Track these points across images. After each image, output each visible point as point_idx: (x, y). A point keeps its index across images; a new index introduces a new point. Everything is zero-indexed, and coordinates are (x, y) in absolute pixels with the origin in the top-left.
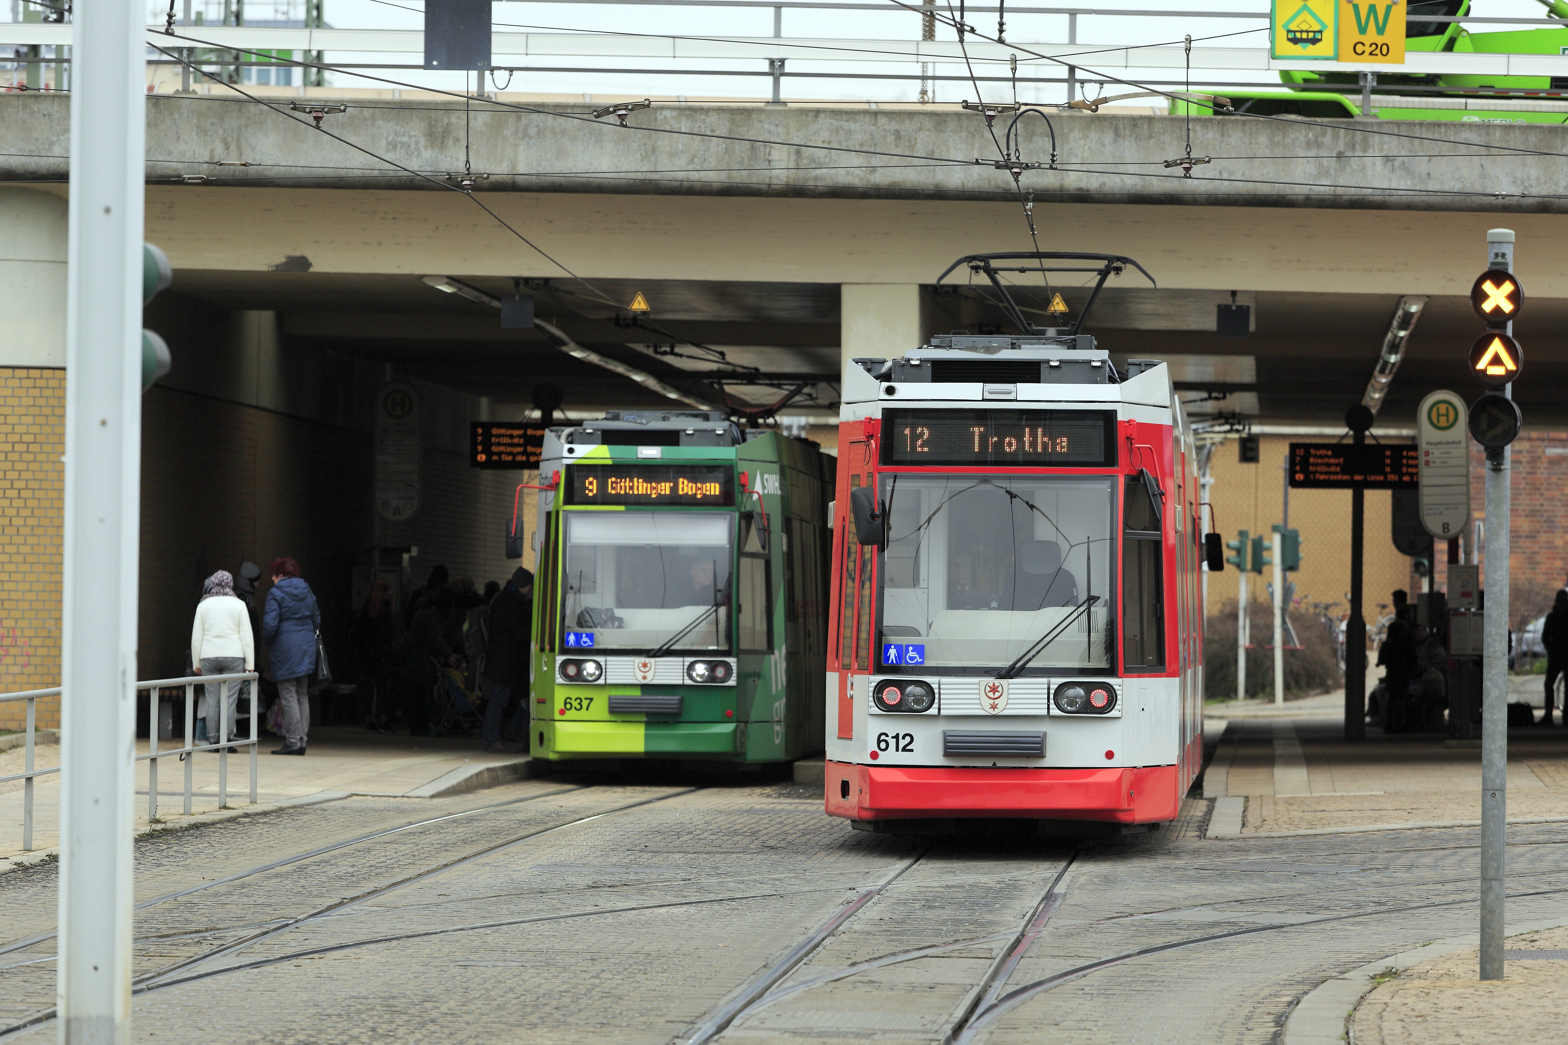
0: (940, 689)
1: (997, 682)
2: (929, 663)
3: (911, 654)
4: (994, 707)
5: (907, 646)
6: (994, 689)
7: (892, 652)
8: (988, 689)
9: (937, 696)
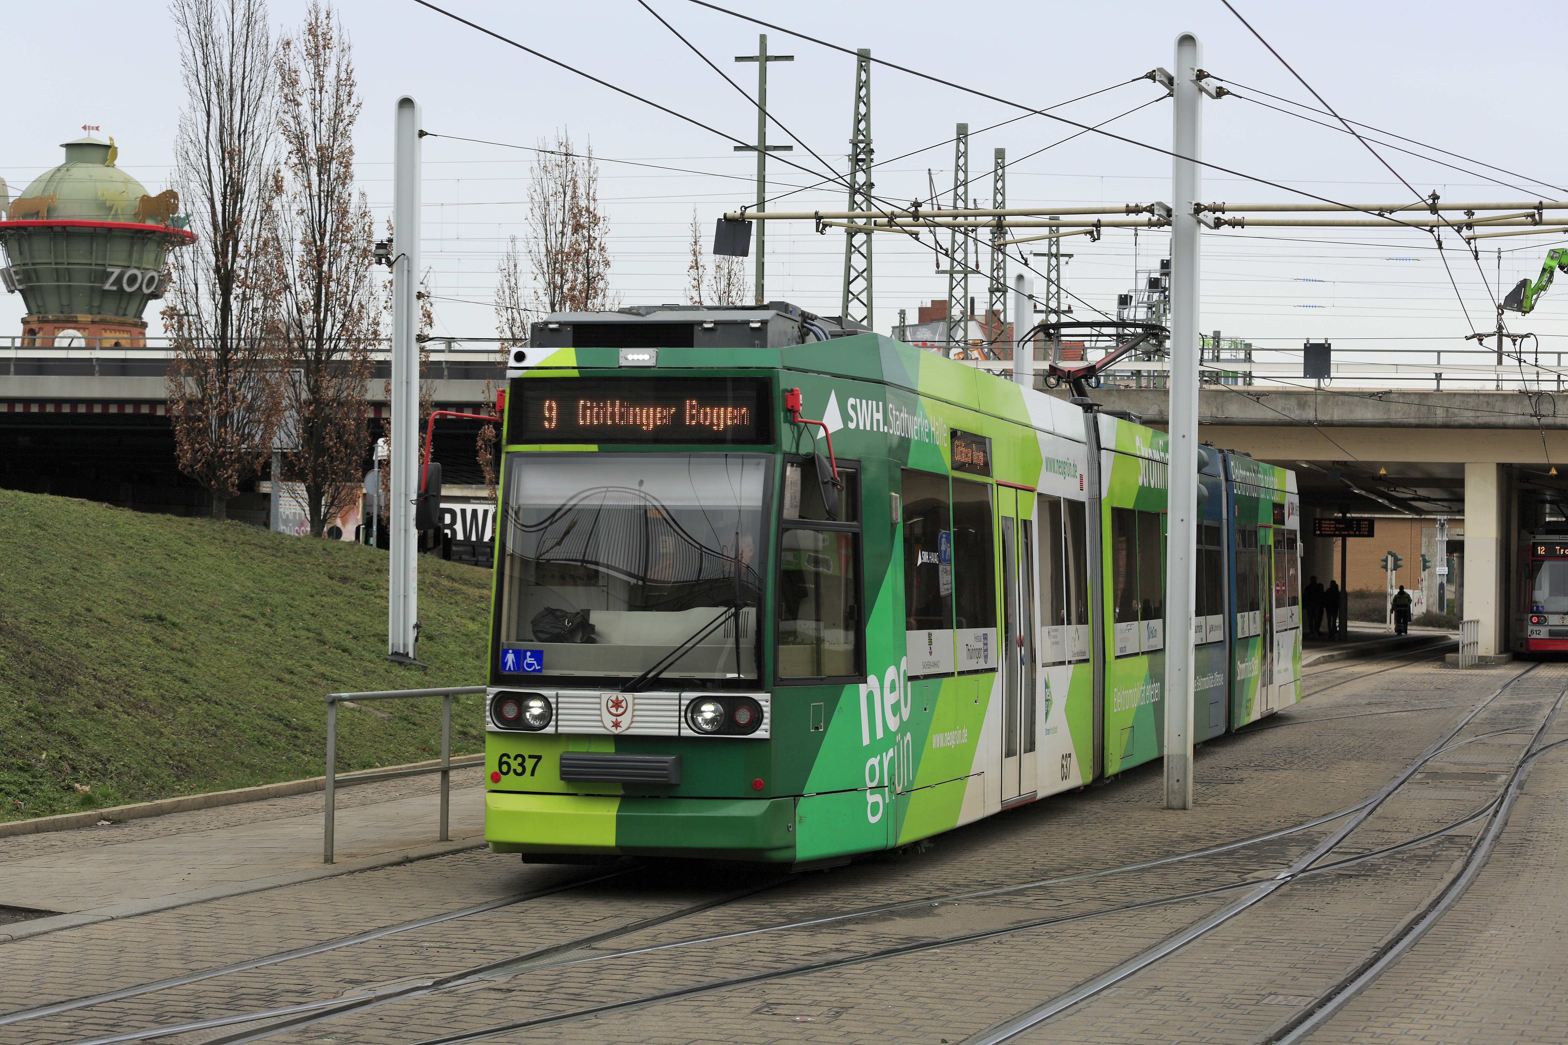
1: (621, 696)
3: (529, 660)
4: (616, 725)
6: (617, 704)
7: (510, 657)
8: (610, 704)
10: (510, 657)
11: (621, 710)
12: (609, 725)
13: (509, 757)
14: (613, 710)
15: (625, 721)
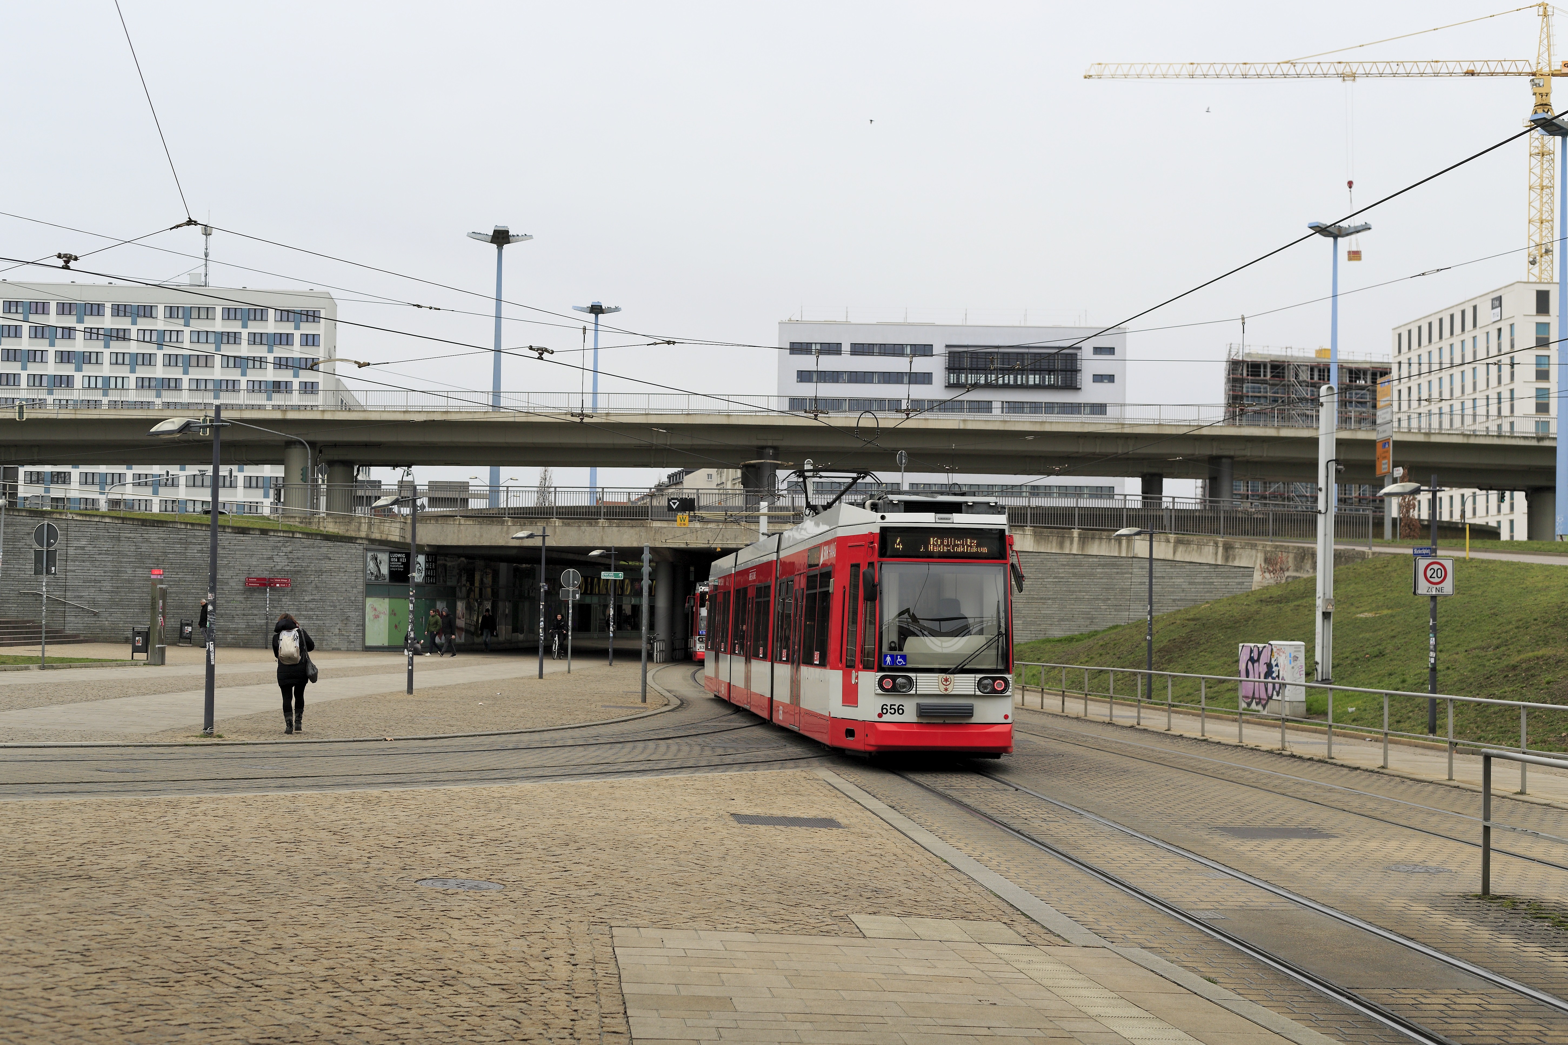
1: (948, 676)
2: (909, 666)
3: (899, 660)
4: (946, 690)
7: (888, 659)
10: (888, 659)
12: (942, 690)
15: (950, 688)
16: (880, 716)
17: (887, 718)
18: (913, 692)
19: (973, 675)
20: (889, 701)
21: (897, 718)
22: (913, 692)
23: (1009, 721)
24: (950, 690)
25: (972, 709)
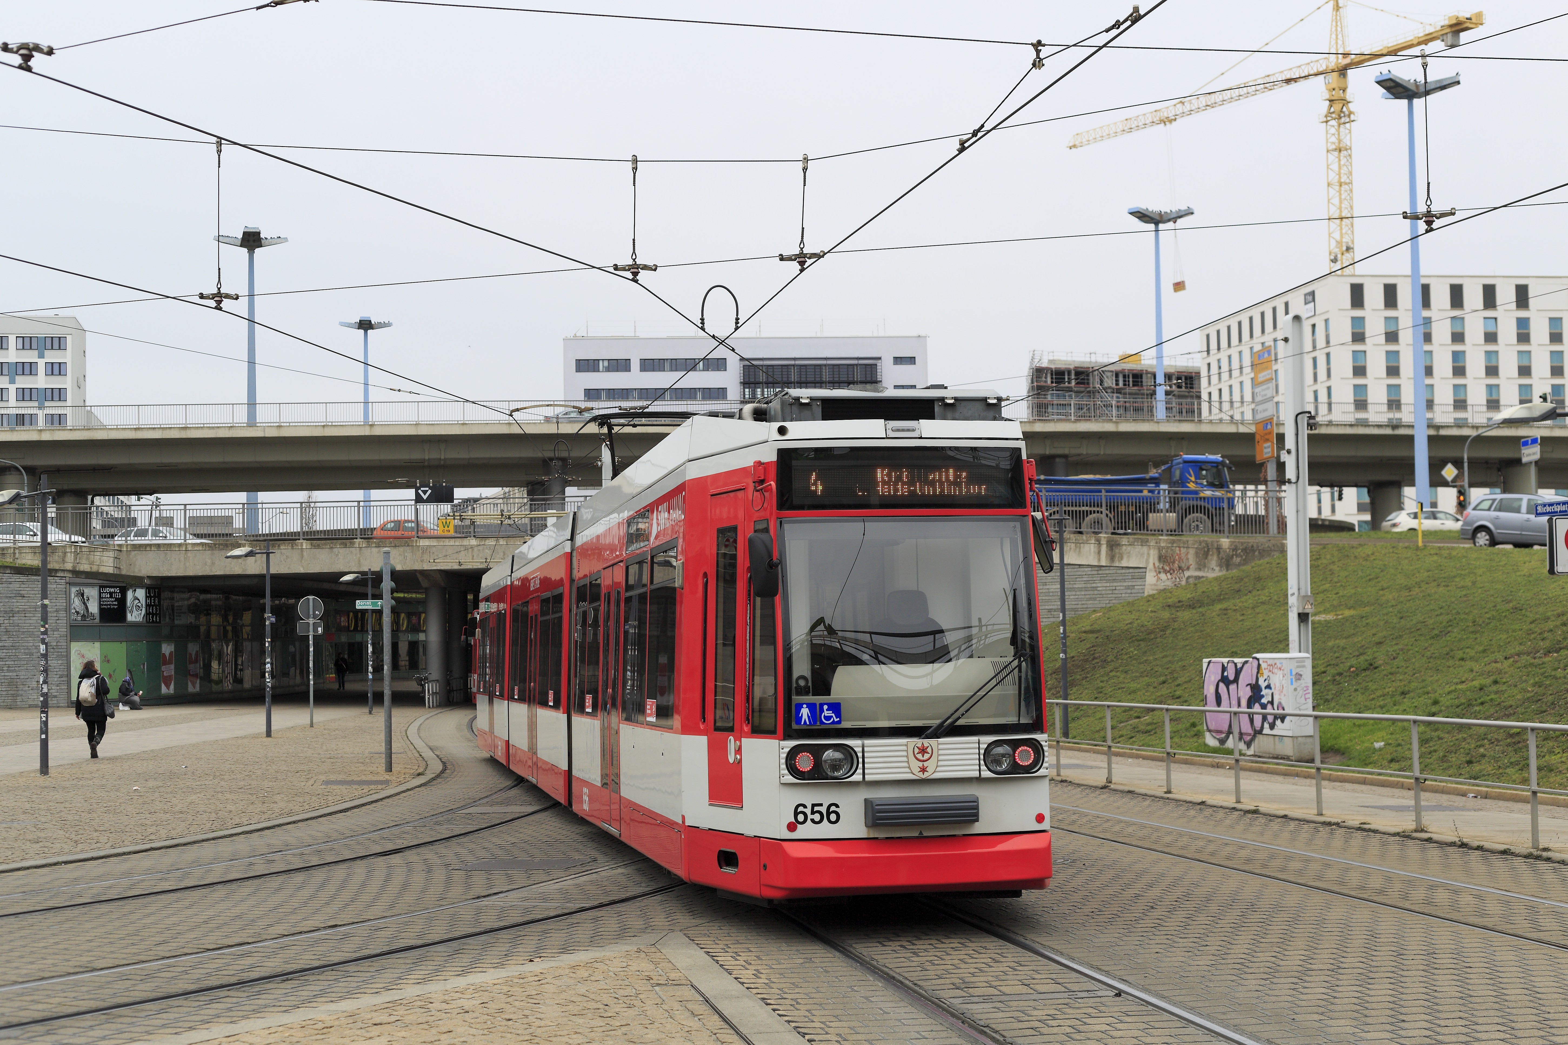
0: (863, 752)
1: (926, 742)
3: (827, 713)
4: (923, 770)
5: (822, 705)
6: (923, 751)
7: (805, 712)
8: (917, 750)
9: (861, 760)
10: (805, 712)
11: (927, 756)
12: (916, 770)
13: (805, 806)
14: (920, 756)
15: (931, 765)
16: (792, 827)
17: (806, 831)
18: (857, 777)
19: (975, 739)
20: (809, 797)
21: (826, 830)
22: (857, 777)
23: (1045, 825)
24: (930, 770)
25: (977, 808)
